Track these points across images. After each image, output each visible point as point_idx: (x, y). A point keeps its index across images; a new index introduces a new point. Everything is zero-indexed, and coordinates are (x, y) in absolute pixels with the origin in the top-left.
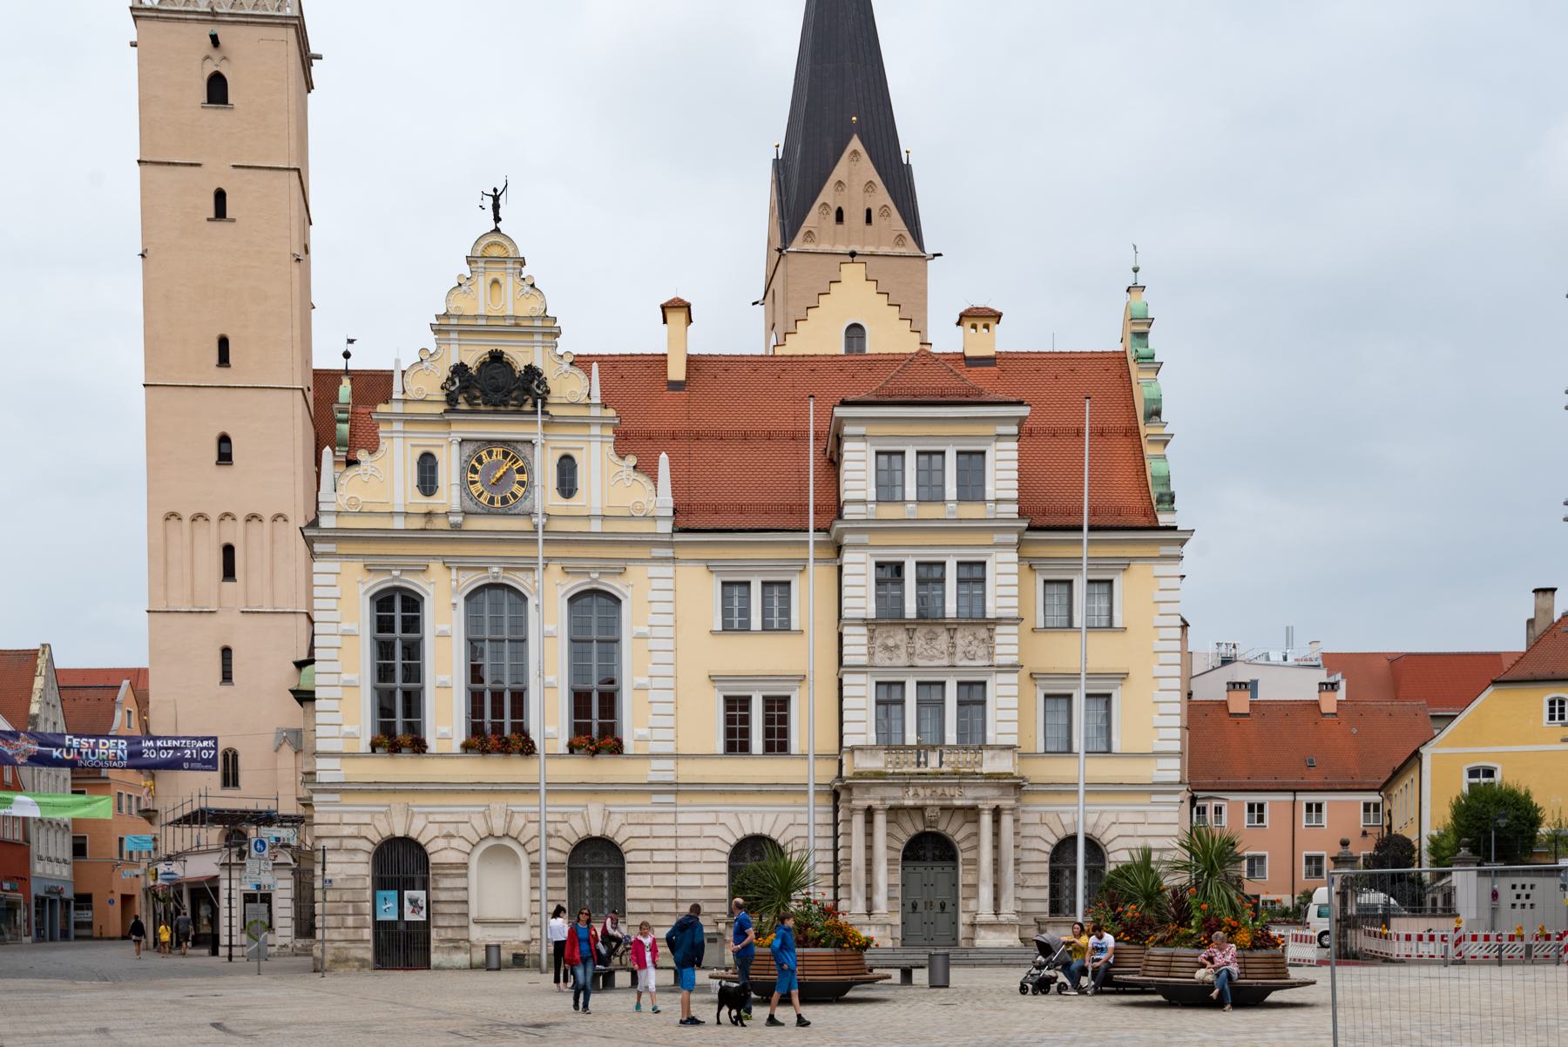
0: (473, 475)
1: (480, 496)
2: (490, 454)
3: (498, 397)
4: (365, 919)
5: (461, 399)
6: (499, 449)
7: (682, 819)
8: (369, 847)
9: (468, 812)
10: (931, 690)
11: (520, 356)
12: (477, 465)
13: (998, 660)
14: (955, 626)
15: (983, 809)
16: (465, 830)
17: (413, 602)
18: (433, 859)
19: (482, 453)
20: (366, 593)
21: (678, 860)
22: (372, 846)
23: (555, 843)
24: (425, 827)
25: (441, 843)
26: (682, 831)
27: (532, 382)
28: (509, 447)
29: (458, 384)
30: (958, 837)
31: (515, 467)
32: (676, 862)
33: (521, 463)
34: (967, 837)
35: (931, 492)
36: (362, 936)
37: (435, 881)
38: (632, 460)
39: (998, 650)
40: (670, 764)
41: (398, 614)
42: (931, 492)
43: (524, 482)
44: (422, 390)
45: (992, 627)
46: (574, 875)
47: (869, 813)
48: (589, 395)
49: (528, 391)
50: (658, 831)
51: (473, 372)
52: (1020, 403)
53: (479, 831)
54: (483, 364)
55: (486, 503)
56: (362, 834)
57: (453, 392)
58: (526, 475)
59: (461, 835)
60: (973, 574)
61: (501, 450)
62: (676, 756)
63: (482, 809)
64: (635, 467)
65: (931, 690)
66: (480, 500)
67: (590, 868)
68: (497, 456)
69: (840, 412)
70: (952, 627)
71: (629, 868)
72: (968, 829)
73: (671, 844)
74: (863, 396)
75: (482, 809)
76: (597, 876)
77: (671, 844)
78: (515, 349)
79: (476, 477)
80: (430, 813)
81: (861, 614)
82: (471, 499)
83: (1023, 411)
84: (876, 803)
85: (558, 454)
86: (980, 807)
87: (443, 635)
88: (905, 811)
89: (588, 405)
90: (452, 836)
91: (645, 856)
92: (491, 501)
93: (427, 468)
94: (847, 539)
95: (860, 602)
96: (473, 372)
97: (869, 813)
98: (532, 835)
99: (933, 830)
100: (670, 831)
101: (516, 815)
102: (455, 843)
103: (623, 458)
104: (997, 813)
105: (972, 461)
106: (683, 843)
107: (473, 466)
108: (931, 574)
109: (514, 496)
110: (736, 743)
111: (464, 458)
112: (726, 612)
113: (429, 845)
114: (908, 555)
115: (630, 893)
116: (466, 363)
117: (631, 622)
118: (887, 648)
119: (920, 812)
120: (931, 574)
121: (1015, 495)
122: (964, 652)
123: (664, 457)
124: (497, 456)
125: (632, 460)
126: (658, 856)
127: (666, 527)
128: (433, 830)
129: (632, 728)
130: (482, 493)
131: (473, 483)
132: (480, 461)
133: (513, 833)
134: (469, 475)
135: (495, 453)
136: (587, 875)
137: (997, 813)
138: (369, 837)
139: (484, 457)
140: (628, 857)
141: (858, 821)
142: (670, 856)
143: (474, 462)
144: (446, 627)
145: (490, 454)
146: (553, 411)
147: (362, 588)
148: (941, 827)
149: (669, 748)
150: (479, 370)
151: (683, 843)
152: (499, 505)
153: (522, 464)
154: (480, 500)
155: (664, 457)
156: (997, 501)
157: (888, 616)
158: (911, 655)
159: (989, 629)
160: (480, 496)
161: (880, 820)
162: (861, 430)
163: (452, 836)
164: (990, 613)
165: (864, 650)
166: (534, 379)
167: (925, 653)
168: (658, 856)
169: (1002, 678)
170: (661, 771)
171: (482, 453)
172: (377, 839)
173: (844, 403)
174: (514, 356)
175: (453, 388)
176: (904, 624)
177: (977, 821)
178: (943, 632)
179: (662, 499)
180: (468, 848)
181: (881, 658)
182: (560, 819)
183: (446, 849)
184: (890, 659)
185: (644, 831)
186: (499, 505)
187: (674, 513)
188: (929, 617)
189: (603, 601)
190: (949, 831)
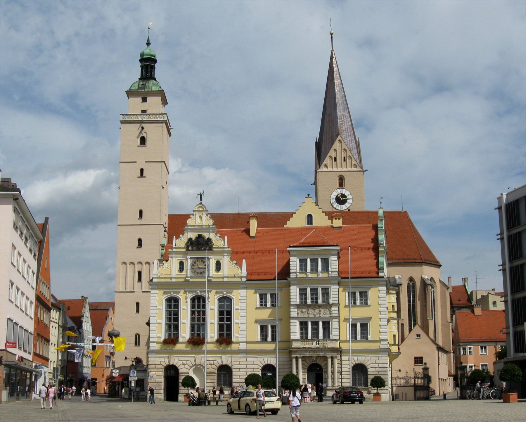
3: (200, 246)
4: (161, 388)
5: (190, 247)
7: (248, 359)
8: (163, 367)
10: (315, 324)
11: (206, 235)
12: (194, 264)
13: (334, 315)
14: (321, 306)
16: (189, 363)
17: (176, 301)
18: (180, 371)
20: (164, 298)
21: (247, 371)
22: (164, 367)
23: (213, 366)
25: (182, 366)
26: (248, 363)
27: (209, 242)
28: (202, 259)
29: (190, 243)
30: (322, 365)
32: (246, 372)
34: (325, 365)
35: (314, 270)
36: (160, 392)
37: (180, 377)
38: (235, 262)
39: (333, 312)
40: (245, 344)
41: (173, 304)
42: (314, 270)
44: (180, 245)
45: (331, 306)
46: (219, 376)
47: (297, 358)
48: (224, 245)
49: (208, 244)
50: (241, 363)
51: (194, 240)
52: (337, 246)
56: (161, 364)
57: (189, 245)
60: (326, 293)
62: (247, 343)
63: (193, 357)
64: (236, 263)
65: (315, 324)
67: (223, 374)
69: (289, 249)
70: (320, 306)
71: (233, 373)
72: (325, 362)
73: (245, 366)
74: (296, 244)
76: (225, 376)
77: (245, 366)
78: (205, 233)
81: (295, 303)
83: (338, 248)
84: (298, 356)
85: (216, 260)
86: (327, 356)
89: (224, 248)
91: (238, 370)
93: (181, 264)
94: (291, 282)
96: (194, 240)
97: (297, 358)
99: (316, 363)
100: (244, 363)
101: (202, 358)
102: (186, 366)
103: (233, 262)
104: (332, 358)
105: (326, 262)
106: (248, 366)
108: (314, 292)
110: (264, 338)
111: (191, 262)
112: (261, 302)
113: (179, 367)
115: (234, 381)
117: (235, 305)
118: (303, 312)
120: (314, 292)
121: (337, 270)
122: (324, 313)
123: (244, 261)
125: (235, 262)
126: (241, 370)
127: (244, 280)
128: (180, 363)
129: (235, 336)
133: (202, 364)
134: (192, 267)
136: (222, 375)
137: (332, 358)
138: (163, 365)
140: (233, 370)
141: (294, 360)
142: (244, 370)
144: (185, 307)
146: (214, 250)
147: (163, 297)
148: (318, 362)
149: (245, 340)
150: (195, 239)
151: (248, 366)
155: (244, 261)
156: (332, 272)
157: (303, 304)
158: (308, 314)
161: (300, 360)
162: (295, 253)
164: (331, 303)
165: (296, 313)
166: (209, 241)
168: (241, 370)
169: (334, 320)
170: (243, 346)
172: (165, 365)
173: (290, 247)
174: (205, 236)
175: (188, 244)
176: (307, 305)
177: (327, 360)
179: (244, 272)
180: (189, 368)
181: (301, 315)
183: (183, 368)
184: (303, 315)
185: (238, 363)
187: (247, 275)
188: (315, 303)
189: (227, 299)
190: (320, 363)
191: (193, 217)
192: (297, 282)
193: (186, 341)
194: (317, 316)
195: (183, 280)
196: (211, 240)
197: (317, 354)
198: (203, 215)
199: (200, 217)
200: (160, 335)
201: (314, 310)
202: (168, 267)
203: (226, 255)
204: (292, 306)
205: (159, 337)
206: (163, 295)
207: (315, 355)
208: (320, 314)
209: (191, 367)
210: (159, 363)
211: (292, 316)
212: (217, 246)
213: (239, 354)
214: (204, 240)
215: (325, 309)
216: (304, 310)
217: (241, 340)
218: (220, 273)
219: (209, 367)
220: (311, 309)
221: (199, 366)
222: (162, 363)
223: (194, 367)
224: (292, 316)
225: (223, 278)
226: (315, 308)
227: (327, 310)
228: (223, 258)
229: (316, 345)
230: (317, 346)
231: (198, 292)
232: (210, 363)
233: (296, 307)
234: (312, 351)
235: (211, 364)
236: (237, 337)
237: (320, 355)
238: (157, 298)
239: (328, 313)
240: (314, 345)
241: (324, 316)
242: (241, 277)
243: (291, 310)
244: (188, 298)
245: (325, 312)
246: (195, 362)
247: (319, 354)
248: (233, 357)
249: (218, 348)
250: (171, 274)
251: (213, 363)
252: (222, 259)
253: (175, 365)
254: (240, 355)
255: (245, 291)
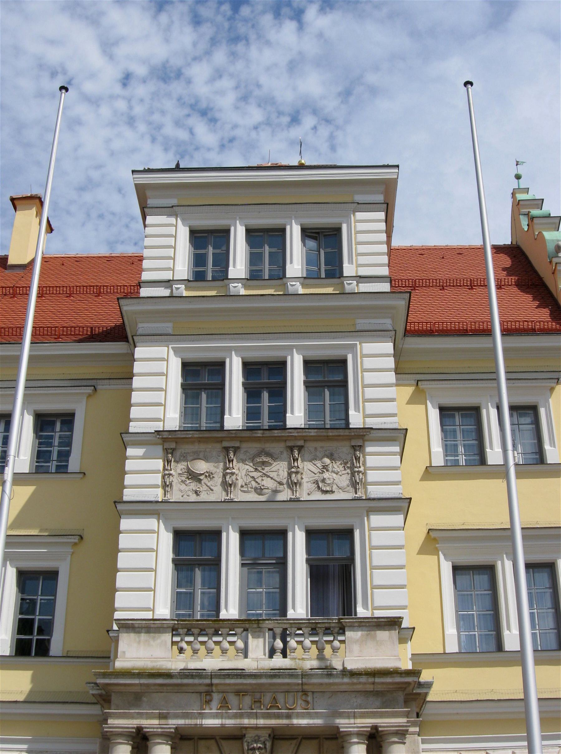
14: (300, 443)
15: (349, 734)
39: (372, 476)
88: (213, 742)
95: (157, 412)
114: (230, 349)
118: (194, 477)
119: (236, 743)
122: (316, 482)
159: (353, 447)
165: (157, 479)
167: (253, 483)
178: (282, 453)
184: (197, 493)
192: (170, 325)
194: (281, 497)
197: (278, 716)
201: (264, 463)
204: (137, 444)
207: (261, 722)
208: (293, 485)
211: (129, 495)
215: (327, 461)
216: (201, 466)
220: (243, 461)
224: (129, 495)
226: (268, 454)
227: (337, 466)
229: (271, 656)
230: (278, 661)
233: (159, 450)
234: (240, 693)
237: (295, 721)
239: (344, 480)
240: (257, 660)
241: (318, 496)
243: (129, 465)
245: (326, 475)
247: (289, 717)
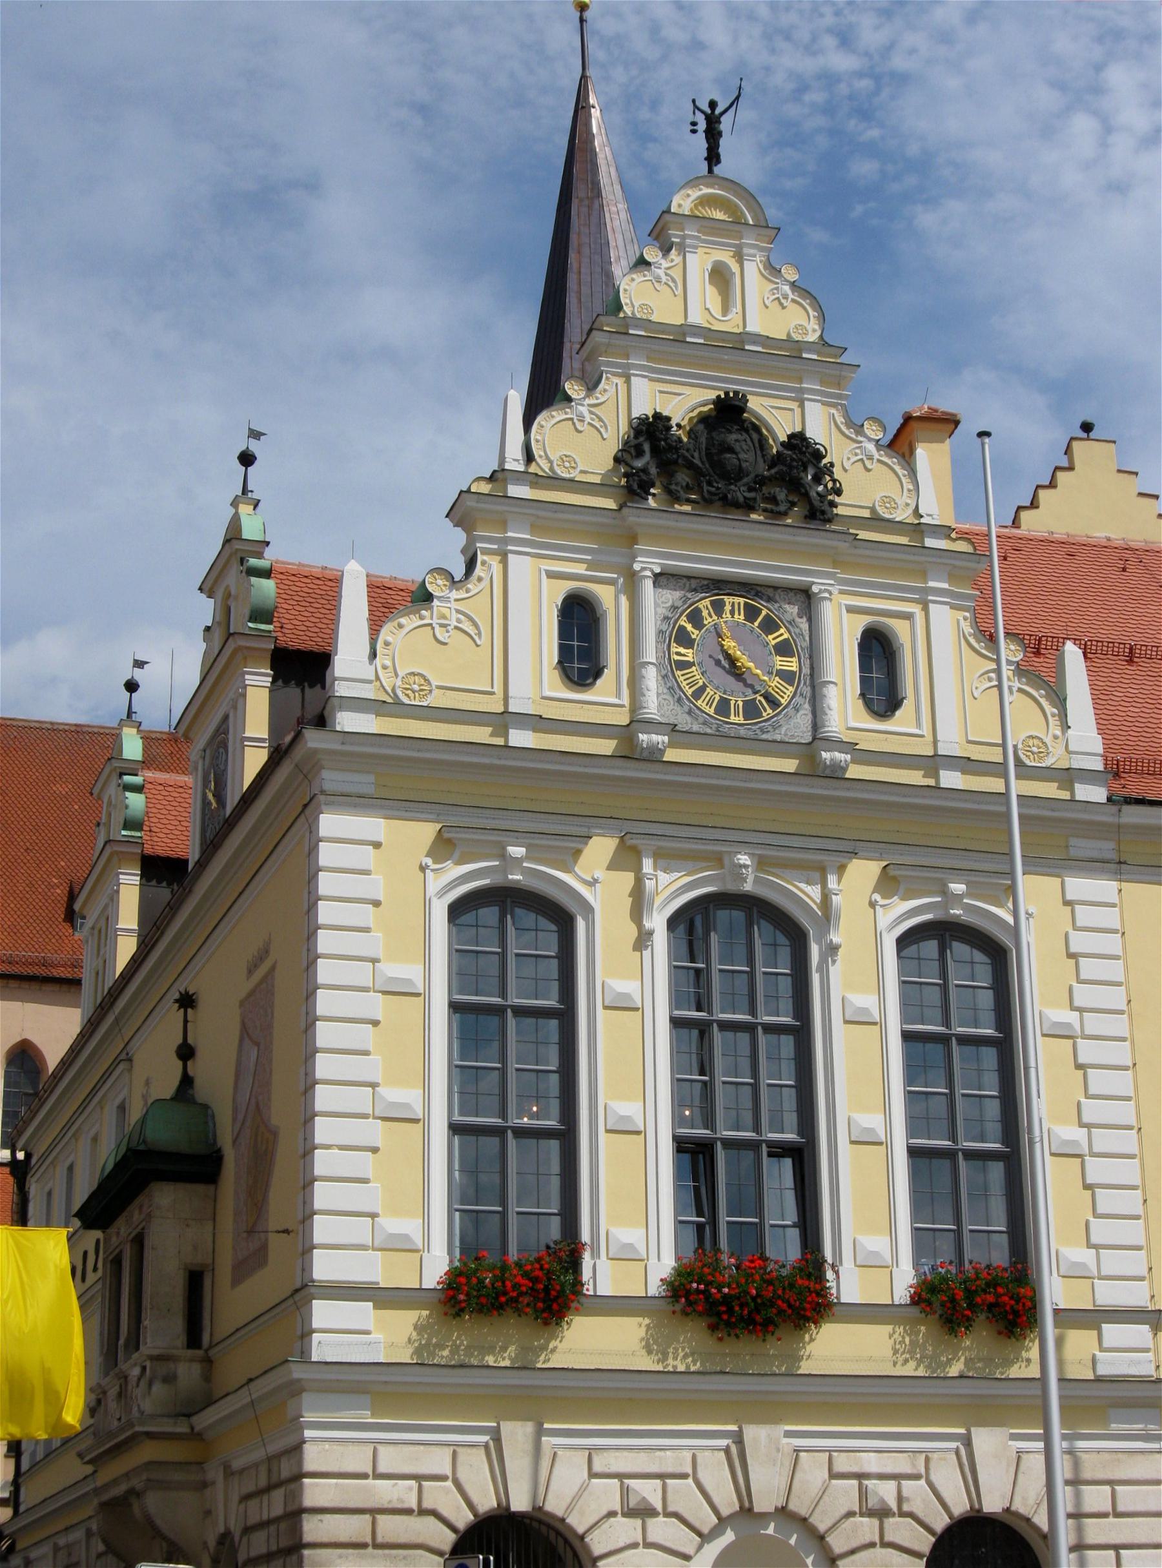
0: (682, 650)
1: (699, 693)
2: (718, 607)
6: (737, 600)
9: (690, 1448)
12: (689, 627)
16: (684, 1496)
19: (701, 605)
24: (583, 1489)
31: (772, 640)
33: (783, 634)
43: (794, 673)
49: (796, 486)
53: (716, 1500)
54: (704, 419)
55: (711, 711)
58: (795, 659)
59: (671, 1509)
61: (742, 600)
66: (699, 703)
68: (732, 613)
75: (723, 1442)
79: (689, 655)
80: (591, 1451)
82: (679, 700)
85: (860, 623)
87: (621, 1006)
90: (650, 1512)
92: (723, 707)
98: (843, 1511)
107: (682, 629)
109: (773, 703)
116: (665, 413)
124: (732, 613)
127: (1096, 794)
130: (702, 689)
131: (683, 665)
132: (696, 618)
133: (798, 1506)
134: (675, 649)
135: (728, 608)
139: (705, 613)
143: (683, 622)
144: (627, 986)
145: (718, 607)
150: (691, 433)
152: (740, 719)
153: (786, 636)
154: (699, 703)
160: (699, 693)
163: (650, 1512)
171: (701, 605)
175: (639, 464)
182: (907, 1469)
186: (740, 719)
191: (665, 264)
193: (655, 1289)
195: (606, 746)
196: (818, 456)
198: (740, 258)
199: (720, 276)
200: (410, 1227)
202: (476, 638)
203: (945, 586)
205: (398, 1246)
206: (429, 861)
209: (705, 1538)
210: (404, 1493)
212: (866, 514)
213: (1106, 1423)
214: (762, 444)
217: (1110, 1295)
218: (902, 720)
219: (867, 1539)
221: (770, 1530)
222: (443, 1498)
223: (729, 1536)
225: (934, 763)
228: (915, 609)
231: (744, 859)
232: (872, 1503)
235: (881, 1513)
236: (1076, 1274)
238: (375, 886)
242: (1068, 777)
244: (658, 901)
246: (744, 1492)
248: (1081, 1444)
249: (933, 1361)
250: (498, 688)
251: (900, 1499)
252: (908, 617)
253: (559, 1513)
254: (1115, 1427)
255: (1103, 888)
